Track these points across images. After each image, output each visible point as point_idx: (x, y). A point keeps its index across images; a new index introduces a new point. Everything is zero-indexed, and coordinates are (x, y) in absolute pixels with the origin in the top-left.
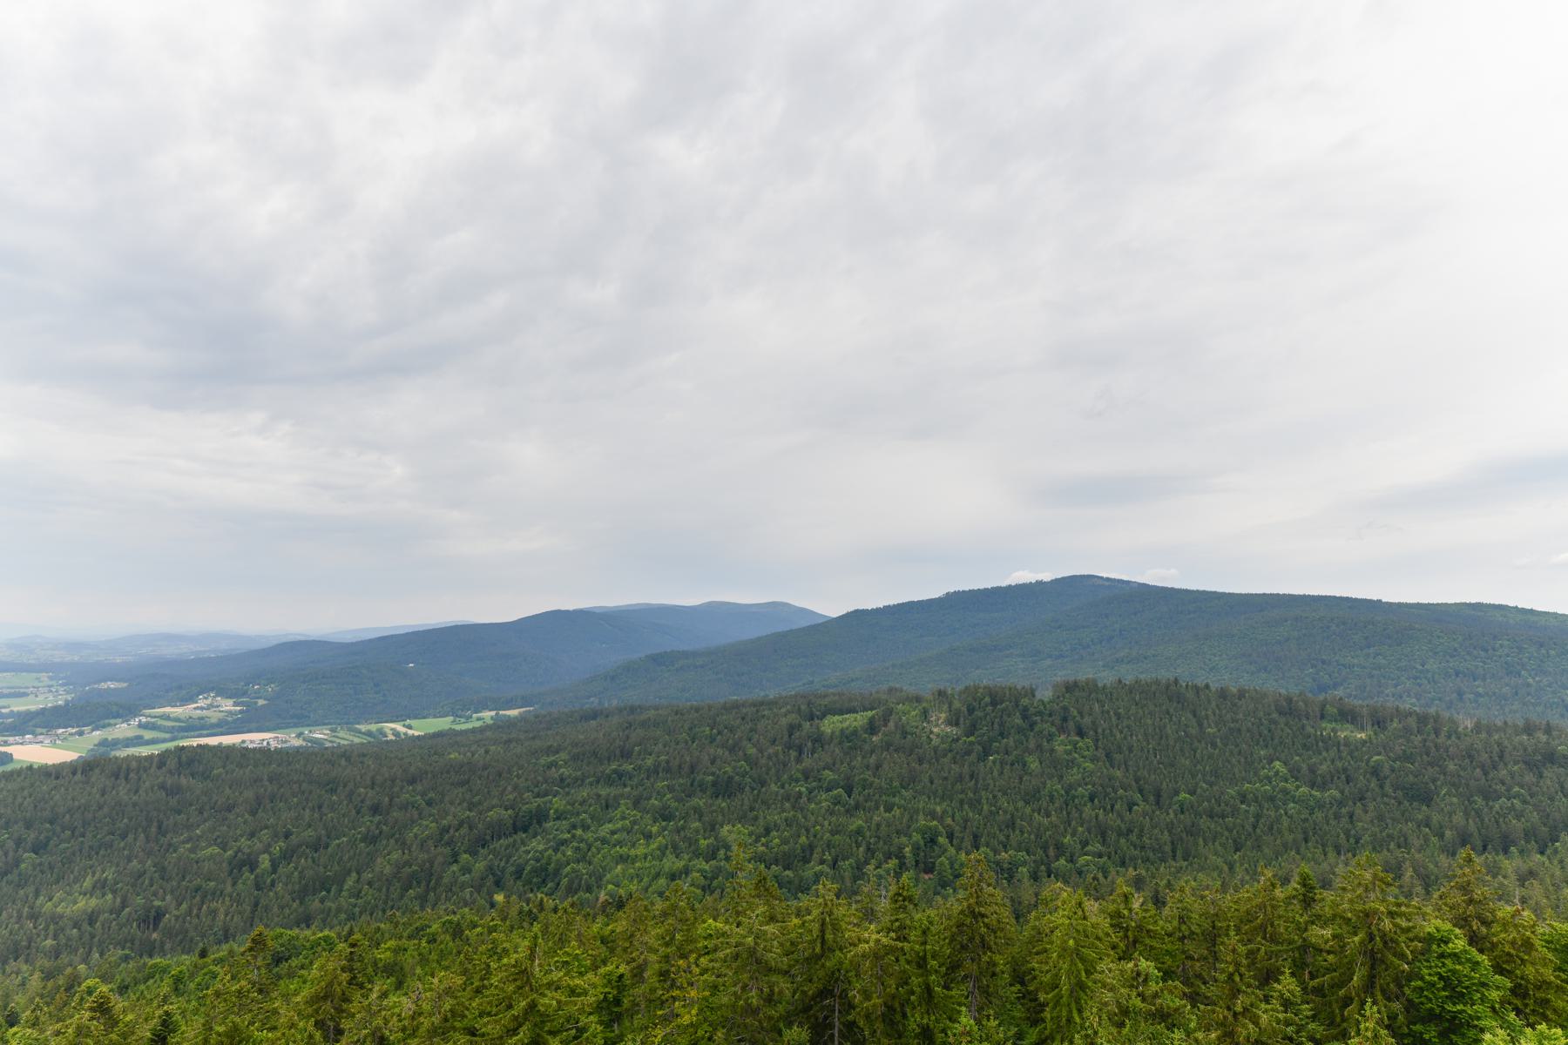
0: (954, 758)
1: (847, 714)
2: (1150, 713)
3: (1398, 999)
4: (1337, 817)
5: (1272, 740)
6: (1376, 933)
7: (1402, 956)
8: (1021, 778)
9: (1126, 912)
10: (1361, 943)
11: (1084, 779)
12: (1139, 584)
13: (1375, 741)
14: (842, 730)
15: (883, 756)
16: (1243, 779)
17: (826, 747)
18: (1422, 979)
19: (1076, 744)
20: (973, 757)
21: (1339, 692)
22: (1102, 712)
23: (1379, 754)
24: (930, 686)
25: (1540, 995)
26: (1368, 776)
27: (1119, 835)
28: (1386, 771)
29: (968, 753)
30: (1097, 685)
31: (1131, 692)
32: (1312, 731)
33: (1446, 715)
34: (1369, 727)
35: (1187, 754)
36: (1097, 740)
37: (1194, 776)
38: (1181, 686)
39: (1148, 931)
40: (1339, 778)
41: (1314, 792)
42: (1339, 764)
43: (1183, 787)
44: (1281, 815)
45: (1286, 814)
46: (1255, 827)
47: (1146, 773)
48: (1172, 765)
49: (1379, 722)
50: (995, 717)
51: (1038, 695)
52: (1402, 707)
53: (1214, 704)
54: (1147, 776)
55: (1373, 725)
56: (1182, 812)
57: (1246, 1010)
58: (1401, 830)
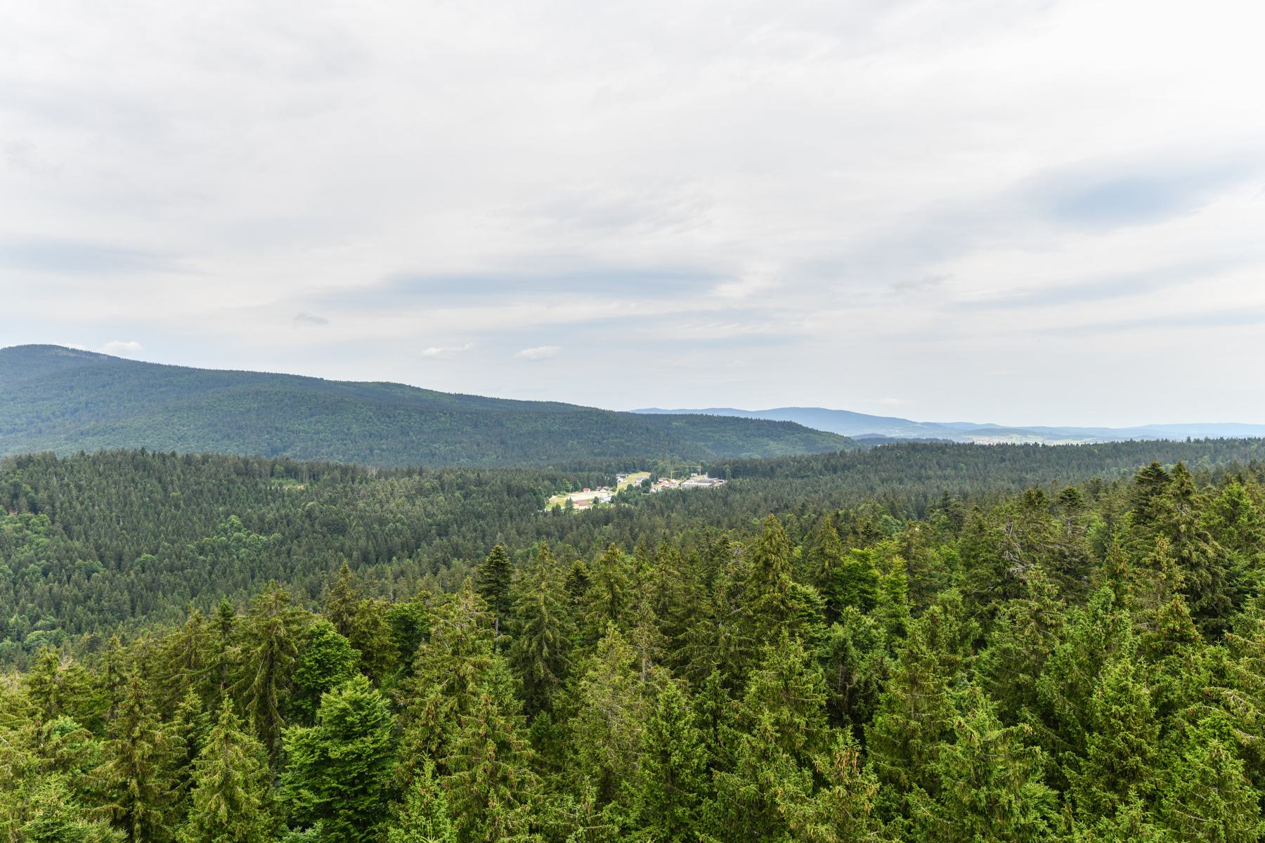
2: (115, 483)
3: (287, 685)
4: (278, 554)
6: (274, 639)
7: (292, 653)
9: (48, 678)
10: (262, 651)
13: (310, 490)
16: (203, 534)
18: (304, 666)
19: (28, 521)
21: (287, 454)
23: (313, 500)
25: (380, 655)
26: (303, 518)
27: (75, 604)
28: (317, 513)
30: (55, 459)
31: (94, 464)
32: (264, 486)
33: (360, 466)
34: (307, 480)
35: (151, 518)
36: (54, 514)
37: (156, 537)
38: (148, 455)
39: (71, 689)
40: (282, 523)
41: (261, 537)
42: (283, 512)
44: (234, 559)
45: (238, 558)
46: (210, 573)
47: (107, 540)
48: (135, 530)
49: (314, 476)
52: (331, 463)
53: (179, 470)
54: (109, 542)
55: (310, 478)
56: (143, 571)
57: (142, 733)
58: (324, 556)
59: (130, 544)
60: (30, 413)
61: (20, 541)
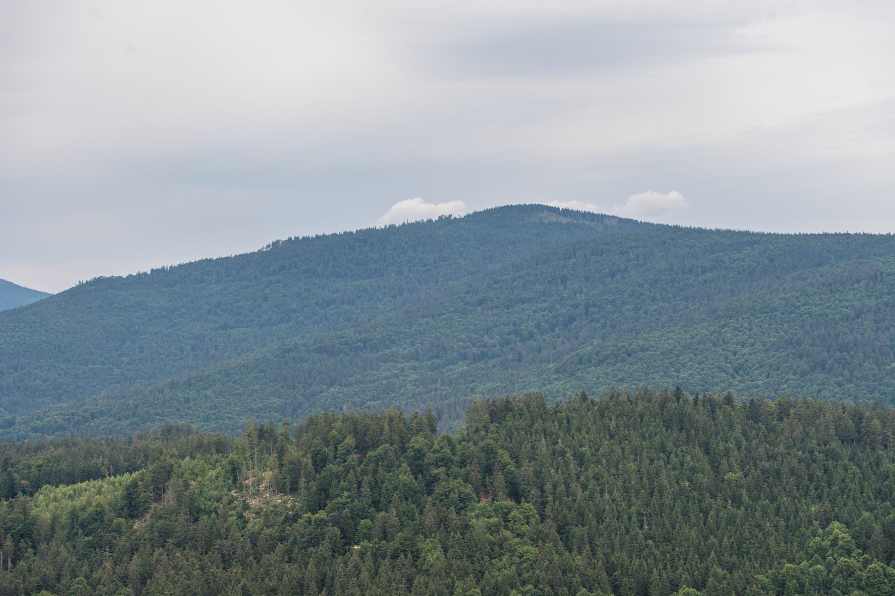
0: (289, 552)
1: (82, 482)
2: (635, 452)
5: (829, 486)
8: (410, 581)
11: (520, 575)
12: (620, 220)
14: (73, 514)
15: (157, 553)
16: (782, 556)
17: (43, 546)
19: (507, 514)
20: (324, 548)
22: (554, 454)
24: (243, 420)
29: (315, 541)
30: (543, 405)
31: (602, 415)
35: (693, 519)
36: (544, 504)
37: (703, 557)
38: (686, 401)
43: (686, 576)
50: (364, 472)
51: (442, 428)
53: (738, 429)
54: (627, 561)
59: (660, 566)
60: (505, 324)
61: (497, 549)
